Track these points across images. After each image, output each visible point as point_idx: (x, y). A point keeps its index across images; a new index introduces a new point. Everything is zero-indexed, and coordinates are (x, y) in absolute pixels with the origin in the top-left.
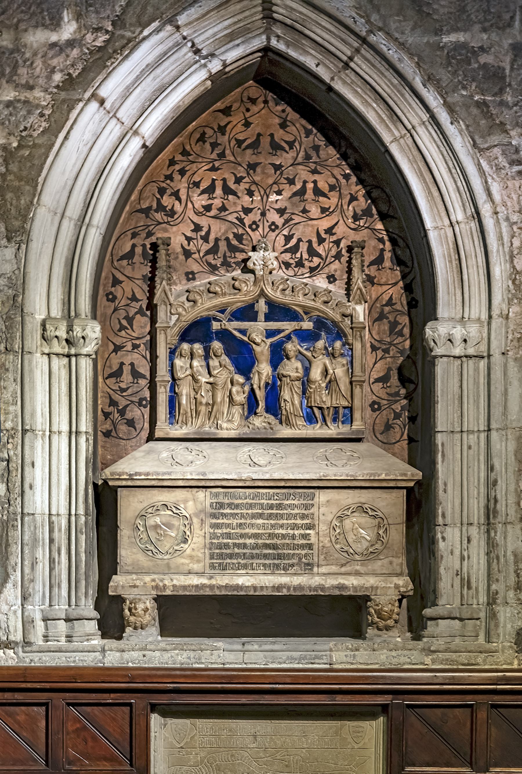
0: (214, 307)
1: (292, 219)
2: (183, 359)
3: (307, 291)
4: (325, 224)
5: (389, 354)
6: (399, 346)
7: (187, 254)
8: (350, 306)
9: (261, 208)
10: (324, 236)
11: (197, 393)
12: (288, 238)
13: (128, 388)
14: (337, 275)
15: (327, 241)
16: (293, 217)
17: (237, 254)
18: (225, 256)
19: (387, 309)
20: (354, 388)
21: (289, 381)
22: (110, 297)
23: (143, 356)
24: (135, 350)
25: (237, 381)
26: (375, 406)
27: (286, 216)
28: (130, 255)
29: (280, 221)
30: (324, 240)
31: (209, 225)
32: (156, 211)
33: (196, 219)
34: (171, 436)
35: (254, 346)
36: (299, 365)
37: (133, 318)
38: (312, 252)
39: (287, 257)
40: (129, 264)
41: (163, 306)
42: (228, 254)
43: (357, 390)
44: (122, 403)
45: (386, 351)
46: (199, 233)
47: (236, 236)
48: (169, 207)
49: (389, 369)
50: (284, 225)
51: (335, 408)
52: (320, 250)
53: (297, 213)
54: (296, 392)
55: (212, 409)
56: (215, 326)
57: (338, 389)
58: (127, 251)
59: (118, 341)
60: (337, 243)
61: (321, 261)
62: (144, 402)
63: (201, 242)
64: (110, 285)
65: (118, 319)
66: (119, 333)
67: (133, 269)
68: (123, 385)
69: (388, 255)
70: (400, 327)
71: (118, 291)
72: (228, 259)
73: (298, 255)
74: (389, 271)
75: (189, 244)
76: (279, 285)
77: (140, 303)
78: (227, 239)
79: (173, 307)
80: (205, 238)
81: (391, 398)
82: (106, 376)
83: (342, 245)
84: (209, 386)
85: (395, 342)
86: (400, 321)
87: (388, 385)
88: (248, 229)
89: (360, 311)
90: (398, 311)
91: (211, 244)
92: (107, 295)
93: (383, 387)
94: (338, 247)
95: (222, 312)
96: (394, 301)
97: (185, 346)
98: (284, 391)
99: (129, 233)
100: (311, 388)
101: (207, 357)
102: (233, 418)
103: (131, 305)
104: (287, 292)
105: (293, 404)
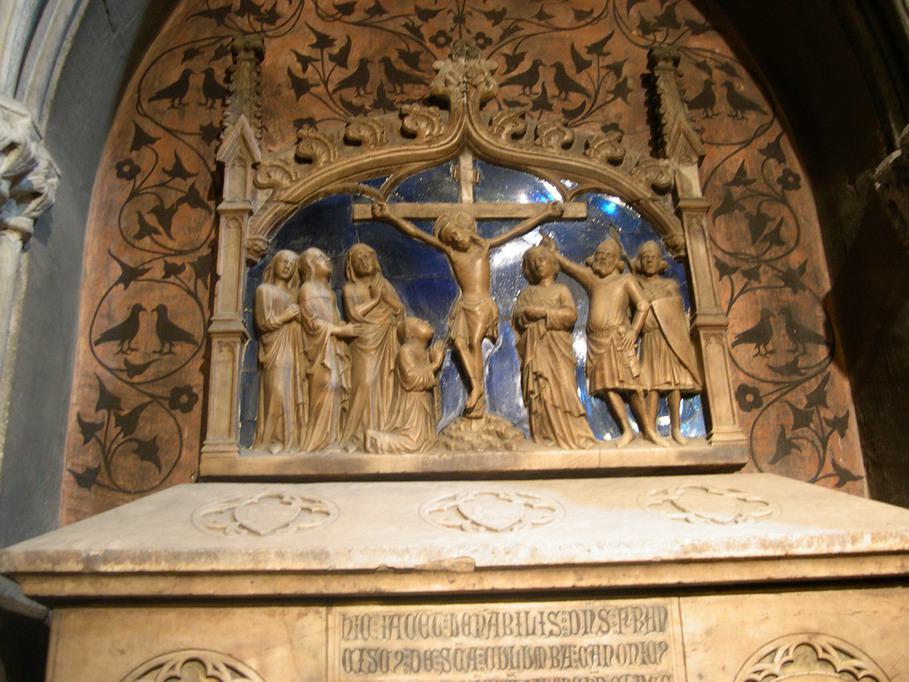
0: (358, 170)
1: (517, 29)
2: (280, 284)
3: (567, 138)
4: (586, 37)
5: (760, 282)
6: (779, 264)
7: (301, 87)
8: (667, 167)
9: (455, 9)
10: (587, 57)
11: (312, 361)
12: (513, 61)
13: (147, 366)
14: (623, 123)
15: (594, 65)
16: (520, 25)
17: (407, 87)
18: (381, 90)
19: (737, 191)
20: (703, 342)
21: (542, 329)
22: (126, 169)
23: (189, 291)
24: (172, 279)
25: (415, 330)
26: (747, 398)
27: (505, 24)
28: (178, 90)
29: (494, 33)
30: (588, 64)
31: (348, 37)
32: (241, 13)
33: (320, 26)
34: (242, 471)
35: (453, 253)
36: (563, 291)
37: (173, 211)
38: (564, 83)
39: (514, 92)
40: (173, 106)
41: (239, 170)
42: (388, 87)
43: (713, 351)
44: (131, 399)
45: (752, 275)
46: (326, 51)
47: (403, 55)
48: (268, 7)
49: (765, 315)
50: (502, 38)
51: (663, 394)
52: (582, 79)
53: (527, 17)
54: (563, 355)
55: (352, 401)
56: (361, 211)
57: (664, 346)
58: (171, 82)
59: (131, 259)
60: (616, 69)
61: (585, 98)
62: (184, 399)
63: (329, 65)
64: (129, 146)
65: (139, 213)
66: (137, 243)
67: (182, 116)
68: (136, 359)
69: (720, 93)
70: (770, 227)
71: (145, 158)
72: (388, 96)
73: (537, 88)
74: (728, 120)
75: (305, 69)
76: (504, 123)
77: (190, 181)
78: (386, 61)
79: (262, 170)
80: (341, 60)
81: (779, 378)
82: (95, 337)
83: (625, 71)
84: (341, 348)
85: (767, 256)
86: (771, 214)
87: (770, 347)
88: (428, 44)
89: (691, 177)
90: (763, 194)
91: (352, 69)
92: (119, 167)
93: (759, 353)
94: (618, 75)
95: (377, 183)
96: (749, 176)
97: (289, 255)
98: (534, 353)
99: (180, 52)
100: (599, 345)
101: (337, 280)
102: (404, 421)
103: (170, 184)
104: (523, 141)
105: (558, 385)
